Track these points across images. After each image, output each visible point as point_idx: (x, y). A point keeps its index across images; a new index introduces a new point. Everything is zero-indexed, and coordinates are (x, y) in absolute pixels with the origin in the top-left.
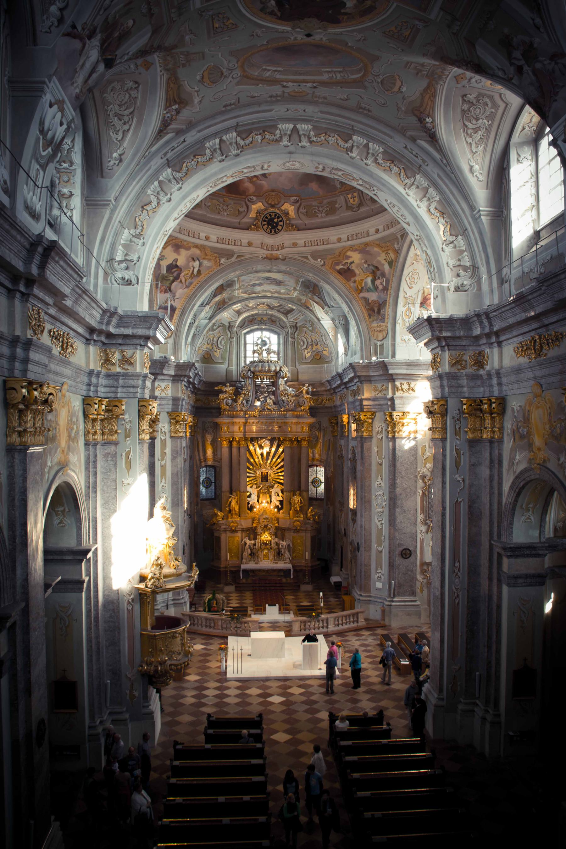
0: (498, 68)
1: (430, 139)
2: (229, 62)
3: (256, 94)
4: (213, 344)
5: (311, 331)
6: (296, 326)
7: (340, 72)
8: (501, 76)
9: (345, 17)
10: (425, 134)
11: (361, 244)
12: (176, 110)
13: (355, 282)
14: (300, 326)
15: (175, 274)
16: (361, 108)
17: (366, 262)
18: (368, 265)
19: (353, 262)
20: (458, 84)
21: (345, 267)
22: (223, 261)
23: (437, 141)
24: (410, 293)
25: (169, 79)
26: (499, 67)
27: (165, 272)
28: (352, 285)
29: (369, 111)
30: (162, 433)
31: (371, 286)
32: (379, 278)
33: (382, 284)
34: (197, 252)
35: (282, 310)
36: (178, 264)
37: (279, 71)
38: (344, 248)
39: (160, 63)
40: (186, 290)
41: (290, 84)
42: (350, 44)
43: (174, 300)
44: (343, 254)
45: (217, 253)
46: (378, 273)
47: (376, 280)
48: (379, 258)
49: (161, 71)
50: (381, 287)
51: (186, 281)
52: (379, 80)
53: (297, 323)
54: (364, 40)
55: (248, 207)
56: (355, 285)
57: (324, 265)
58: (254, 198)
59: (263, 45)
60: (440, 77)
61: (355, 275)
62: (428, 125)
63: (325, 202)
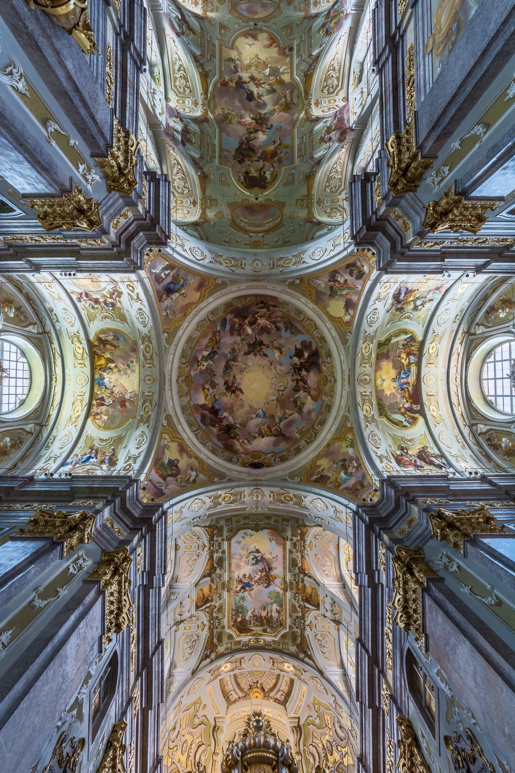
3: (238, 240)
4: (188, 756)
5: (319, 727)
6: (299, 726)
11: (324, 448)
13: (331, 483)
14: (304, 725)
15: (174, 472)
16: (286, 242)
17: (334, 463)
18: (337, 463)
19: (324, 469)
21: (319, 476)
22: (216, 479)
24: (380, 452)
27: (166, 462)
28: (329, 486)
29: (289, 242)
30: (75, 562)
31: (346, 477)
32: (349, 466)
33: (353, 467)
34: (197, 464)
35: (278, 696)
36: (179, 465)
38: (313, 459)
40: (179, 488)
41: (252, 234)
43: (166, 488)
44: (313, 465)
45: (212, 472)
46: (347, 463)
47: (347, 469)
48: (342, 451)
50: (354, 470)
51: (181, 482)
53: (299, 718)
55: (238, 460)
56: (332, 484)
57: (301, 480)
58: (243, 456)
61: (329, 478)
63: (292, 450)
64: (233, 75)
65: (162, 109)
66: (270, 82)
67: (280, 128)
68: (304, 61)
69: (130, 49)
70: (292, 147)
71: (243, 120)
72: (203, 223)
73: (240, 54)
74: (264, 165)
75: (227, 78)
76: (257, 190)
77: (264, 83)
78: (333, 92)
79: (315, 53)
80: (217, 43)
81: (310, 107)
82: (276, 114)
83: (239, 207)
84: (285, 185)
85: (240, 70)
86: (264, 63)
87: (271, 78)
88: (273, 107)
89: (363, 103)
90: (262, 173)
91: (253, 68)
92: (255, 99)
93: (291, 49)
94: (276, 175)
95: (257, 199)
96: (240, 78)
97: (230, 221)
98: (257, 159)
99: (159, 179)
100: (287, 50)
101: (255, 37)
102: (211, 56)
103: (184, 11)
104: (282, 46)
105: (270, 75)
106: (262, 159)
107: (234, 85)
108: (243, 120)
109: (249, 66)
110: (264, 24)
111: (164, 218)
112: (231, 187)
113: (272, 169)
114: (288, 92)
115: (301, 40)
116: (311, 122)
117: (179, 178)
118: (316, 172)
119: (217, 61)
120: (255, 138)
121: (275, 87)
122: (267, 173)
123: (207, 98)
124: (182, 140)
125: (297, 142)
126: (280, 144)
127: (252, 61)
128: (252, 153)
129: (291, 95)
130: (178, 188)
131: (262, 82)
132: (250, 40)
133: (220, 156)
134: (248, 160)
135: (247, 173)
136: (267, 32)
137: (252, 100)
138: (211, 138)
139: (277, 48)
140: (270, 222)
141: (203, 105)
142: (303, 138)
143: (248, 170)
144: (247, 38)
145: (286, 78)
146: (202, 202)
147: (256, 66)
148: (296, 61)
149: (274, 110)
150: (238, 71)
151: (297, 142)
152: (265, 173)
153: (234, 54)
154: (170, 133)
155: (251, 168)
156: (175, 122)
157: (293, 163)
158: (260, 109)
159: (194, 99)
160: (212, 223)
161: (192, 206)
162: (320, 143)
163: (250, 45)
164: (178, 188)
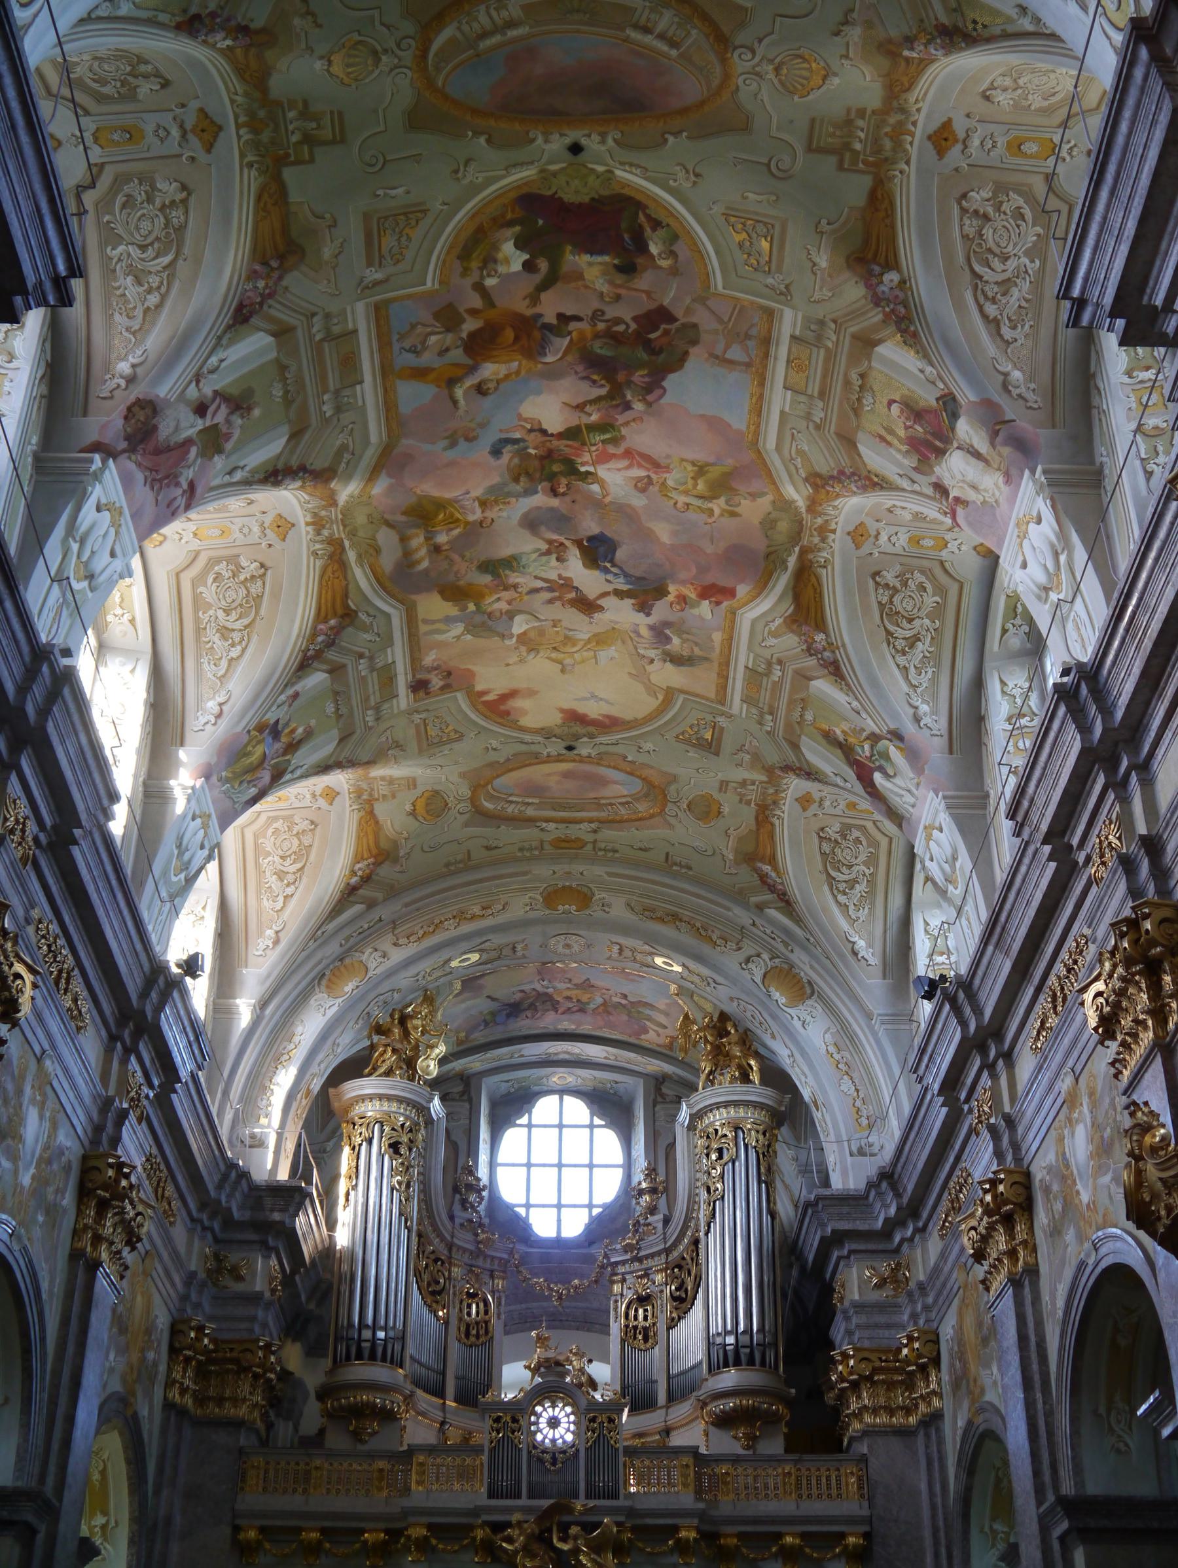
0: (222, 361)
1: (193, 10)
2: (756, 95)
7: (484, 35)
8: (210, 361)
9: (509, 216)
10: (212, 6)
12: (912, 49)
20: (201, 110)
23: (179, 27)
25: (909, 89)
26: (224, 364)
37: (636, 27)
39: (912, 135)
42: (482, 140)
49: (919, 110)
52: (384, 58)
54: (456, 171)
59: (676, 134)
60: (252, 114)
62: (219, 36)
64: (671, 618)
65: (1023, 536)
66: (506, 595)
67: (453, 444)
68: (361, 656)
69: (1105, 730)
70: (387, 372)
71: (642, 473)
72: (909, 41)
73: (641, 676)
74: (534, 299)
75: (705, 608)
76: (574, 192)
77: (536, 590)
78: (213, 562)
79: (317, 679)
80: (736, 704)
81: (315, 515)
82: (478, 492)
83: (684, 111)
84: (414, 213)
85: (644, 632)
86: (530, 651)
87: (503, 606)
88: (489, 514)
89: (75, 547)
90: (543, 265)
91: (586, 637)
92: (579, 543)
93: (419, 686)
94: (465, 255)
95: (576, 149)
96: (644, 608)
97: (740, 38)
98: (573, 325)
99: (1113, 315)
100: (436, 682)
101: (574, 717)
102: (768, 673)
103: (858, 788)
104: (459, 696)
105: (511, 615)
106: (547, 327)
107: (672, 588)
108: (642, 473)
109: (600, 640)
110: (534, 748)
111: (1140, 138)
112: (718, 209)
113: (490, 282)
114: (425, 564)
115: (377, 709)
116: (303, 469)
117: (1005, 258)
118: (253, 275)
119: (742, 658)
120: (580, 407)
121: (487, 579)
122: (516, 266)
123: (804, 552)
124: (954, 416)
125: (368, 391)
126: (452, 382)
127: (592, 653)
128: (600, 349)
129: (407, 554)
130: (1019, 215)
131: (547, 595)
132: (593, 710)
133: (766, 342)
134: (618, 321)
135: (628, 269)
136: (523, 729)
137: (591, 539)
138: (808, 417)
139: (479, 687)
140: (496, 30)
141: (824, 531)
142: (338, 409)
143: (620, 279)
144: (608, 717)
145: (432, 606)
146: (898, 145)
147: (568, 640)
148: (398, 655)
149: (483, 504)
150: (652, 628)
151: (368, 391)
152: (528, 266)
153: (667, 675)
154: (1006, 451)
155: (602, 285)
156: (974, 487)
157: (380, 312)
158: (552, 509)
159: (866, 548)
160: (855, 34)
161: (959, 127)
162: (249, 393)
163: (593, 696)
164: (1019, 215)
